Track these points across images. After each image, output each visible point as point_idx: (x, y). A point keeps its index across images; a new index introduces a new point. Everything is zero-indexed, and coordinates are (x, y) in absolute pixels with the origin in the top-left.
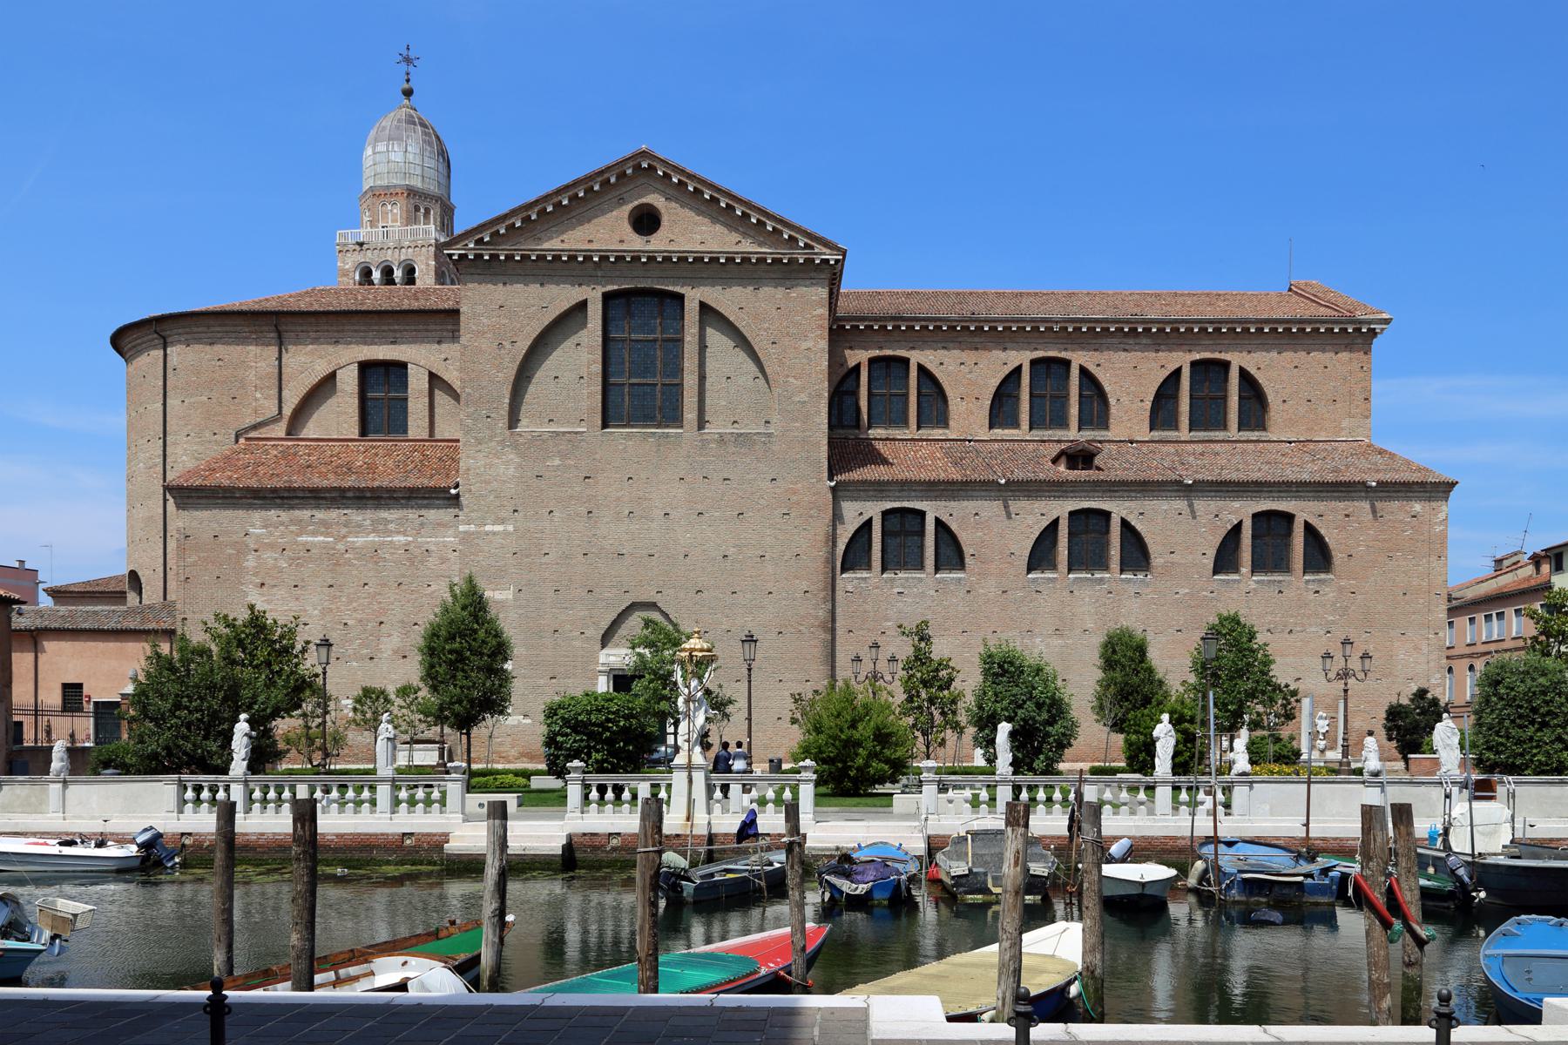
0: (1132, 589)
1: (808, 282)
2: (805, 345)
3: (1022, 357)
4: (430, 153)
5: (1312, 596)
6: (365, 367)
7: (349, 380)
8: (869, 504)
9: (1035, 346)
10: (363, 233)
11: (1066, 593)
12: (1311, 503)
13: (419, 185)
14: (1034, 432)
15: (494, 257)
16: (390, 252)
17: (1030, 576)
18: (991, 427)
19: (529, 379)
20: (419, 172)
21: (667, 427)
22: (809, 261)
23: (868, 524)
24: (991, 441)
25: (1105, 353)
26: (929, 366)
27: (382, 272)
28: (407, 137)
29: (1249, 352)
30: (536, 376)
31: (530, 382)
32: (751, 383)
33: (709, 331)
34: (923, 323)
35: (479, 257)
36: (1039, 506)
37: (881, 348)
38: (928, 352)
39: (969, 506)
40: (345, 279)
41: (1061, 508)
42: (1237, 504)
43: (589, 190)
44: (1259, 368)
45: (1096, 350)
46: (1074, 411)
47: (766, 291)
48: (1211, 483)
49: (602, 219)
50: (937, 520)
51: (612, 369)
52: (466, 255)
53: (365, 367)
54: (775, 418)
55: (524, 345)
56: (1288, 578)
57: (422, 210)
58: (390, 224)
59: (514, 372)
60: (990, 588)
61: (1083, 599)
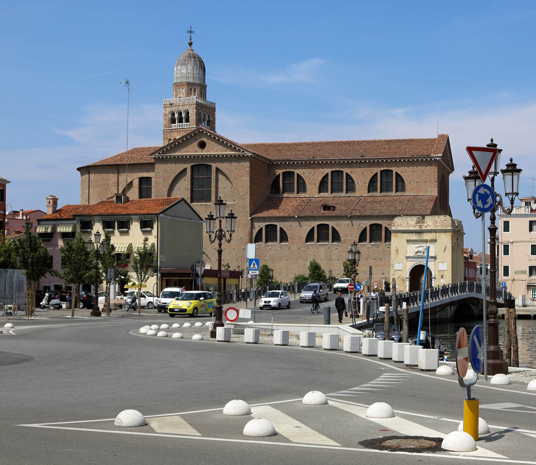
0: (335, 247)
1: (244, 161)
2: (243, 179)
3: (328, 171)
4: (196, 68)
5: (387, 249)
6: (141, 179)
7: (136, 183)
8: (261, 223)
9: (332, 167)
10: (172, 100)
11: (316, 249)
12: (387, 221)
13: (192, 81)
14: (333, 194)
15: (163, 157)
16: (181, 107)
17: (306, 244)
18: (320, 192)
19: (173, 190)
20: (192, 76)
21: (208, 202)
22: (243, 156)
23: (261, 229)
24: (318, 197)
25: (354, 169)
26: (300, 174)
27: (178, 114)
28: (188, 64)
29: (399, 167)
30: (175, 188)
31: (173, 190)
32: (230, 189)
33: (219, 175)
34: (297, 161)
35: (159, 157)
36: (309, 223)
37: (286, 169)
38: (300, 170)
39: (289, 223)
40: (166, 117)
41: (315, 224)
42: (365, 222)
43: (187, 138)
44: (402, 172)
45: (351, 168)
46: (345, 187)
47: (233, 164)
48: (357, 216)
49: (191, 145)
50: (280, 228)
51: (194, 186)
52: (156, 157)
53: (141, 179)
54: (236, 199)
55: (171, 181)
56: (380, 244)
57: (193, 90)
58: (182, 96)
59: (168, 188)
60: (295, 247)
61: (321, 250)
